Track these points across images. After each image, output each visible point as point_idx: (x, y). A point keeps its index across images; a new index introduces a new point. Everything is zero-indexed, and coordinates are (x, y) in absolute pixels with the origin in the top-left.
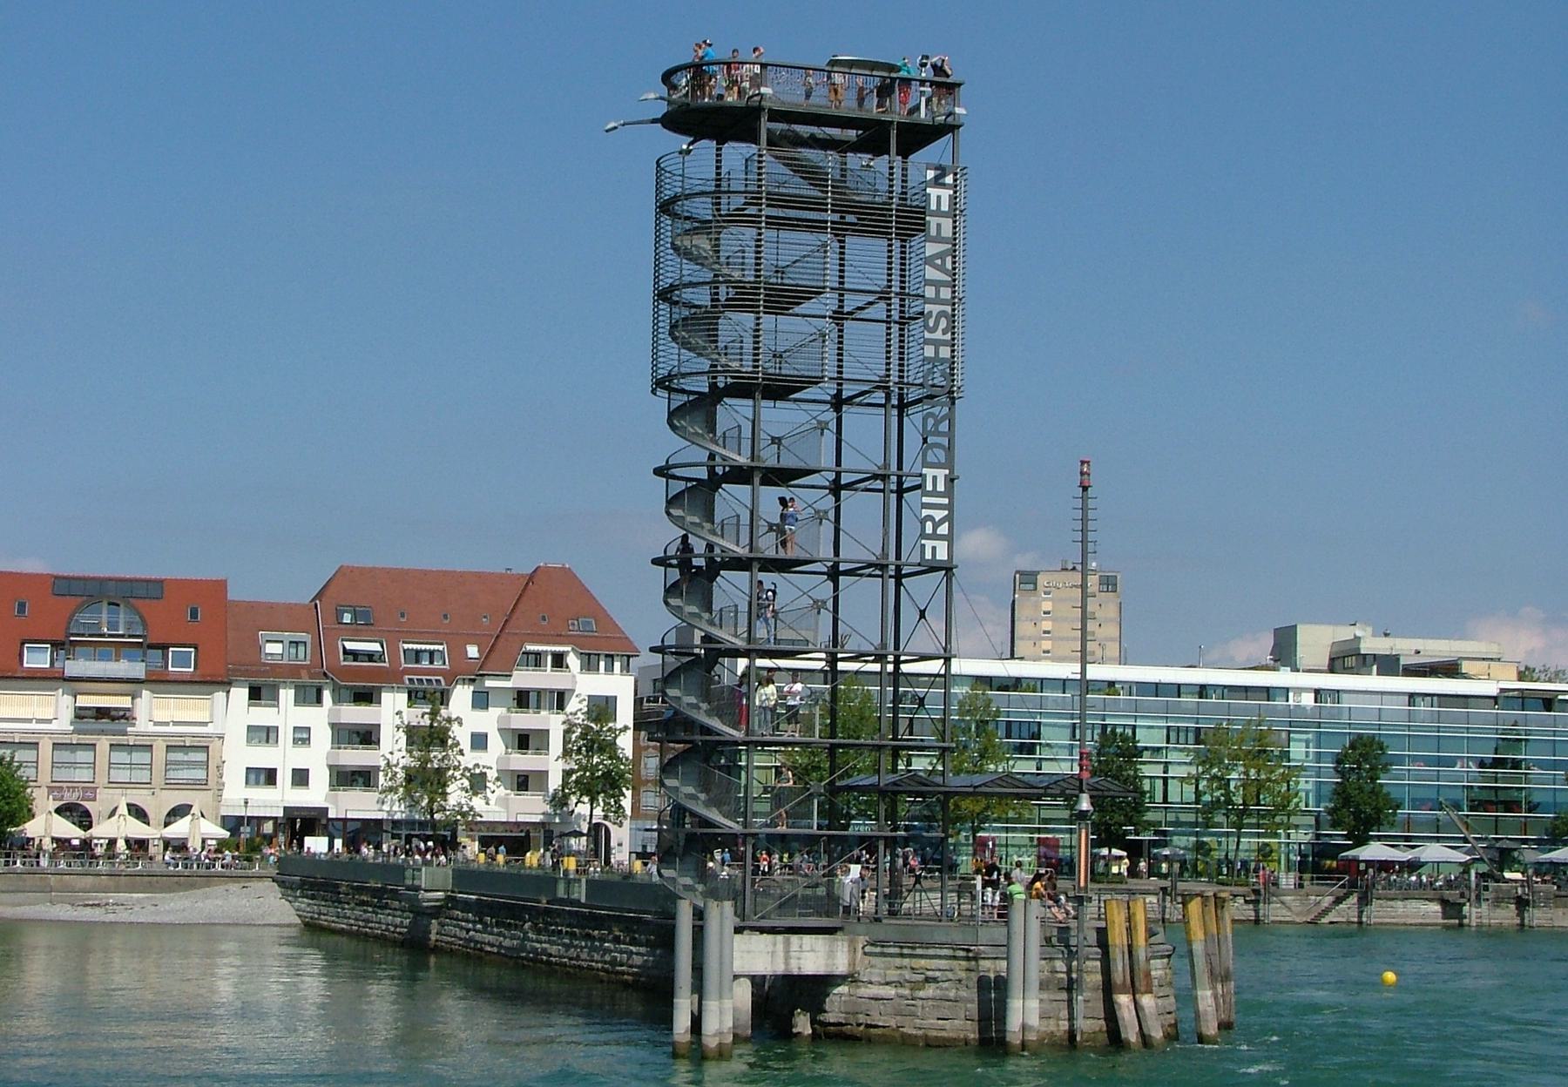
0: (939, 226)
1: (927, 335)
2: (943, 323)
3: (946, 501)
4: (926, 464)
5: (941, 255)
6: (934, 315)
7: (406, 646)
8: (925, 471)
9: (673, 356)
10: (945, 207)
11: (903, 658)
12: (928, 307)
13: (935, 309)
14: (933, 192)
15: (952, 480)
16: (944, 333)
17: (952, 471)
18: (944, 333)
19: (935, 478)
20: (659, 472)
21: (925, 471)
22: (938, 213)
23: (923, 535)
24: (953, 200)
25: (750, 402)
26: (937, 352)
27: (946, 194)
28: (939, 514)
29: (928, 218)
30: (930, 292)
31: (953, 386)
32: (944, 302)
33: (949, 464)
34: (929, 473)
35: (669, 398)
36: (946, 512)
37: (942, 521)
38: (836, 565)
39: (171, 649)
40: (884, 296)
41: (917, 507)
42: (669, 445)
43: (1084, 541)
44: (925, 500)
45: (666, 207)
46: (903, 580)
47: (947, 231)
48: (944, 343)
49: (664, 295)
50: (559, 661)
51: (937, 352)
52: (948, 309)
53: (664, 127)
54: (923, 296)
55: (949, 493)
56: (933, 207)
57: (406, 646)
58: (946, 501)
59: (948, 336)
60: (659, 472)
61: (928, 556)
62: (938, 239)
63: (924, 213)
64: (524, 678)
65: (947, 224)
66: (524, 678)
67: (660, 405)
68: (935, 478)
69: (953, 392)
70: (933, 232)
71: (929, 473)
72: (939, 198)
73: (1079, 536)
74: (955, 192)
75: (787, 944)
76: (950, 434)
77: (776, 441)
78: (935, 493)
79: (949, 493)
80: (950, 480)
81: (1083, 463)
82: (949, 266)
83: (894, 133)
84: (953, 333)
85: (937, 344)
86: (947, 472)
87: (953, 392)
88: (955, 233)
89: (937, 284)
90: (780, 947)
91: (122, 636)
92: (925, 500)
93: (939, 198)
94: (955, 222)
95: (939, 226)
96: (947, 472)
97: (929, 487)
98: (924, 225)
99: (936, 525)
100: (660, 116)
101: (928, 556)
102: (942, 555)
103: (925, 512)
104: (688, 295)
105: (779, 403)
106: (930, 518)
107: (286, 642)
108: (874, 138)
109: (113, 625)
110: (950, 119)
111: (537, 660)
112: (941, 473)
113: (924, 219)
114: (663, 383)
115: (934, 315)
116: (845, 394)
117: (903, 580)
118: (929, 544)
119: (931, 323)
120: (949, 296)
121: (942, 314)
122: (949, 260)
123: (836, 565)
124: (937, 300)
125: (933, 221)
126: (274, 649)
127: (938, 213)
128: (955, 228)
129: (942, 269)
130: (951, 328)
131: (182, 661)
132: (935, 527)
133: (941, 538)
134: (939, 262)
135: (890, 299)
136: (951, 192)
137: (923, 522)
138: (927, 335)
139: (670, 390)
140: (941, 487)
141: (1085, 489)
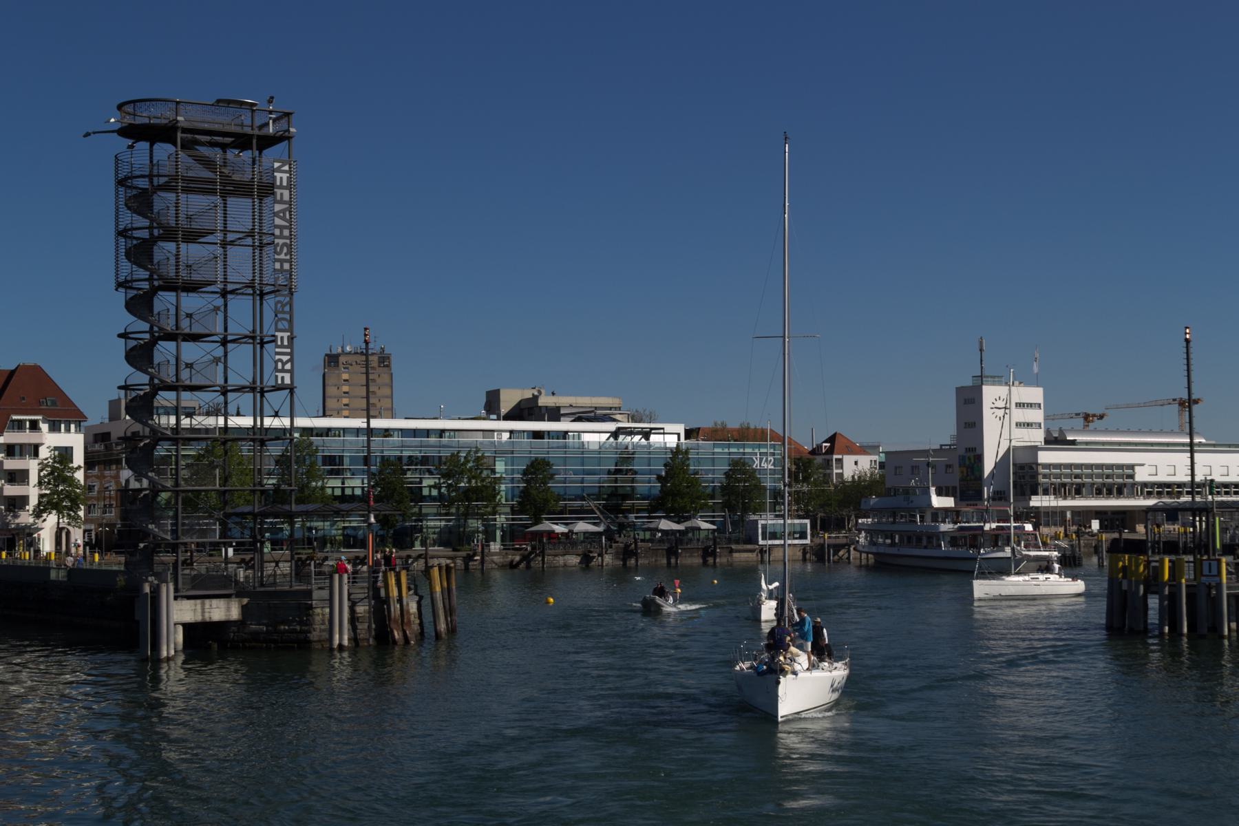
0: (282, 194)
1: (276, 257)
2: (285, 250)
3: (289, 350)
5: (283, 211)
8: (277, 334)
9: (128, 218)
10: (285, 183)
11: (266, 389)
13: (281, 241)
15: (292, 338)
16: (286, 255)
17: (292, 333)
18: (286, 255)
20: (120, 336)
21: (277, 334)
22: (281, 187)
23: (277, 370)
24: (289, 179)
25: (174, 294)
27: (285, 176)
28: (285, 358)
30: (277, 232)
32: (285, 238)
33: (291, 330)
34: (279, 334)
35: (126, 293)
36: (288, 357)
37: (287, 362)
38: (225, 337)
40: (251, 234)
41: (273, 354)
44: (277, 350)
45: (121, 182)
46: (265, 394)
47: (286, 197)
48: (286, 261)
49: (122, 233)
53: (119, 135)
55: (291, 345)
56: (278, 183)
58: (289, 350)
59: (288, 257)
60: (120, 336)
61: (280, 382)
62: (281, 202)
63: (273, 187)
65: (286, 193)
67: (121, 297)
68: (282, 338)
70: (278, 198)
71: (279, 334)
72: (281, 178)
74: (291, 175)
76: (291, 312)
77: (189, 316)
78: (282, 346)
79: (291, 345)
80: (291, 339)
81: (366, 329)
82: (288, 217)
83: (254, 141)
85: (282, 261)
88: (291, 198)
89: (281, 228)
92: (277, 350)
93: (281, 178)
94: (291, 192)
96: (289, 334)
97: (279, 343)
99: (284, 364)
100: (116, 128)
101: (280, 382)
102: (287, 381)
103: (278, 357)
104: (137, 234)
105: (190, 294)
106: (280, 360)
108: (242, 141)
110: (287, 134)
112: (286, 335)
114: (121, 285)
116: (228, 239)
117: (265, 394)
118: (280, 375)
119: (278, 249)
120: (288, 234)
121: (285, 244)
122: (287, 213)
123: (225, 337)
124: (281, 237)
125: (278, 192)
128: (291, 195)
129: (283, 218)
130: (290, 252)
132: (283, 366)
133: (287, 371)
134: (282, 215)
135: (254, 236)
137: (276, 362)
138: (276, 257)
139: (126, 288)
140: (286, 343)
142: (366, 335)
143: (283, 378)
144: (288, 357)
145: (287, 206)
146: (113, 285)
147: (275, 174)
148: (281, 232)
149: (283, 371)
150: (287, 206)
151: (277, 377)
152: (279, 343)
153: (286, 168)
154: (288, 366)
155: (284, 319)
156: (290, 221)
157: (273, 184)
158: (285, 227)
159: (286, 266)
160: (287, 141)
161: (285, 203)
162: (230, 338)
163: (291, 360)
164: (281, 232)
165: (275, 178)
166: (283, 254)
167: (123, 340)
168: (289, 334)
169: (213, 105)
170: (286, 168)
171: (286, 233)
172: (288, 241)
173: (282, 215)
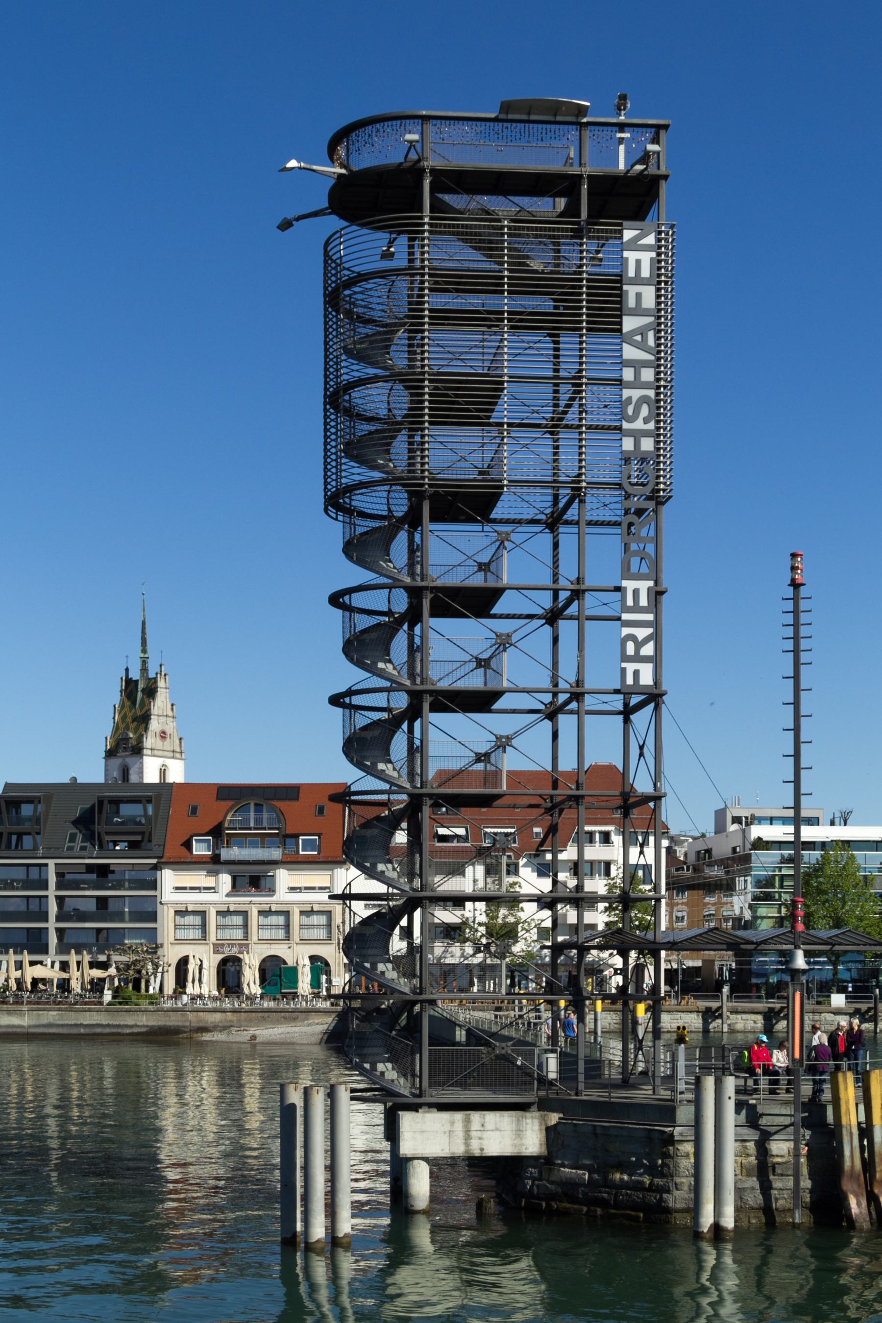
0: (639, 296)
2: (645, 411)
3: (650, 617)
5: (642, 331)
6: (634, 401)
8: (625, 583)
10: (645, 273)
13: (635, 394)
16: (646, 421)
18: (646, 421)
19: (636, 592)
21: (625, 583)
22: (638, 280)
23: (626, 658)
24: (656, 264)
26: (637, 444)
27: (646, 258)
28: (642, 633)
29: (625, 287)
30: (628, 374)
31: (658, 484)
32: (646, 386)
36: (650, 631)
37: (646, 640)
48: (646, 434)
51: (637, 444)
52: (651, 393)
54: (621, 380)
56: (631, 273)
58: (650, 617)
59: (651, 426)
61: (630, 681)
62: (638, 311)
63: (620, 282)
65: (649, 295)
68: (636, 592)
69: (658, 491)
70: (631, 303)
71: (629, 585)
72: (638, 262)
74: (659, 254)
78: (636, 609)
80: (657, 594)
81: (794, 556)
82: (651, 341)
84: (658, 422)
85: (637, 435)
86: (651, 583)
87: (658, 491)
88: (659, 303)
89: (637, 365)
93: (638, 262)
94: (658, 290)
96: (651, 583)
97: (630, 602)
98: (620, 296)
99: (639, 645)
101: (630, 681)
102: (647, 678)
103: (626, 631)
106: (632, 638)
110: (651, 170)
112: (644, 586)
113: (620, 289)
115: (634, 401)
118: (630, 667)
121: (644, 399)
122: (651, 335)
124: (637, 384)
125: (631, 291)
128: (658, 297)
130: (656, 415)
133: (645, 659)
136: (653, 254)
140: (644, 602)
141: (795, 585)
142: (793, 568)
143: (636, 673)
144: (650, 631)
145: (652, 319)
147: (626, 254)
148: (637, 375)
149: (638, 658)
150: (652, 319)
151: (623, 671)
152: (630, 602)
157: (621, 276)
158: (645, 364)
159: (647, 444)
161: (645, 313)
163: (656, 637)
164: (637, 375)
165: (624, 262)
166: (640, 420)
169: (496, 120)
170: (650, 240)
171: (648, 375)
173: (638, 338)
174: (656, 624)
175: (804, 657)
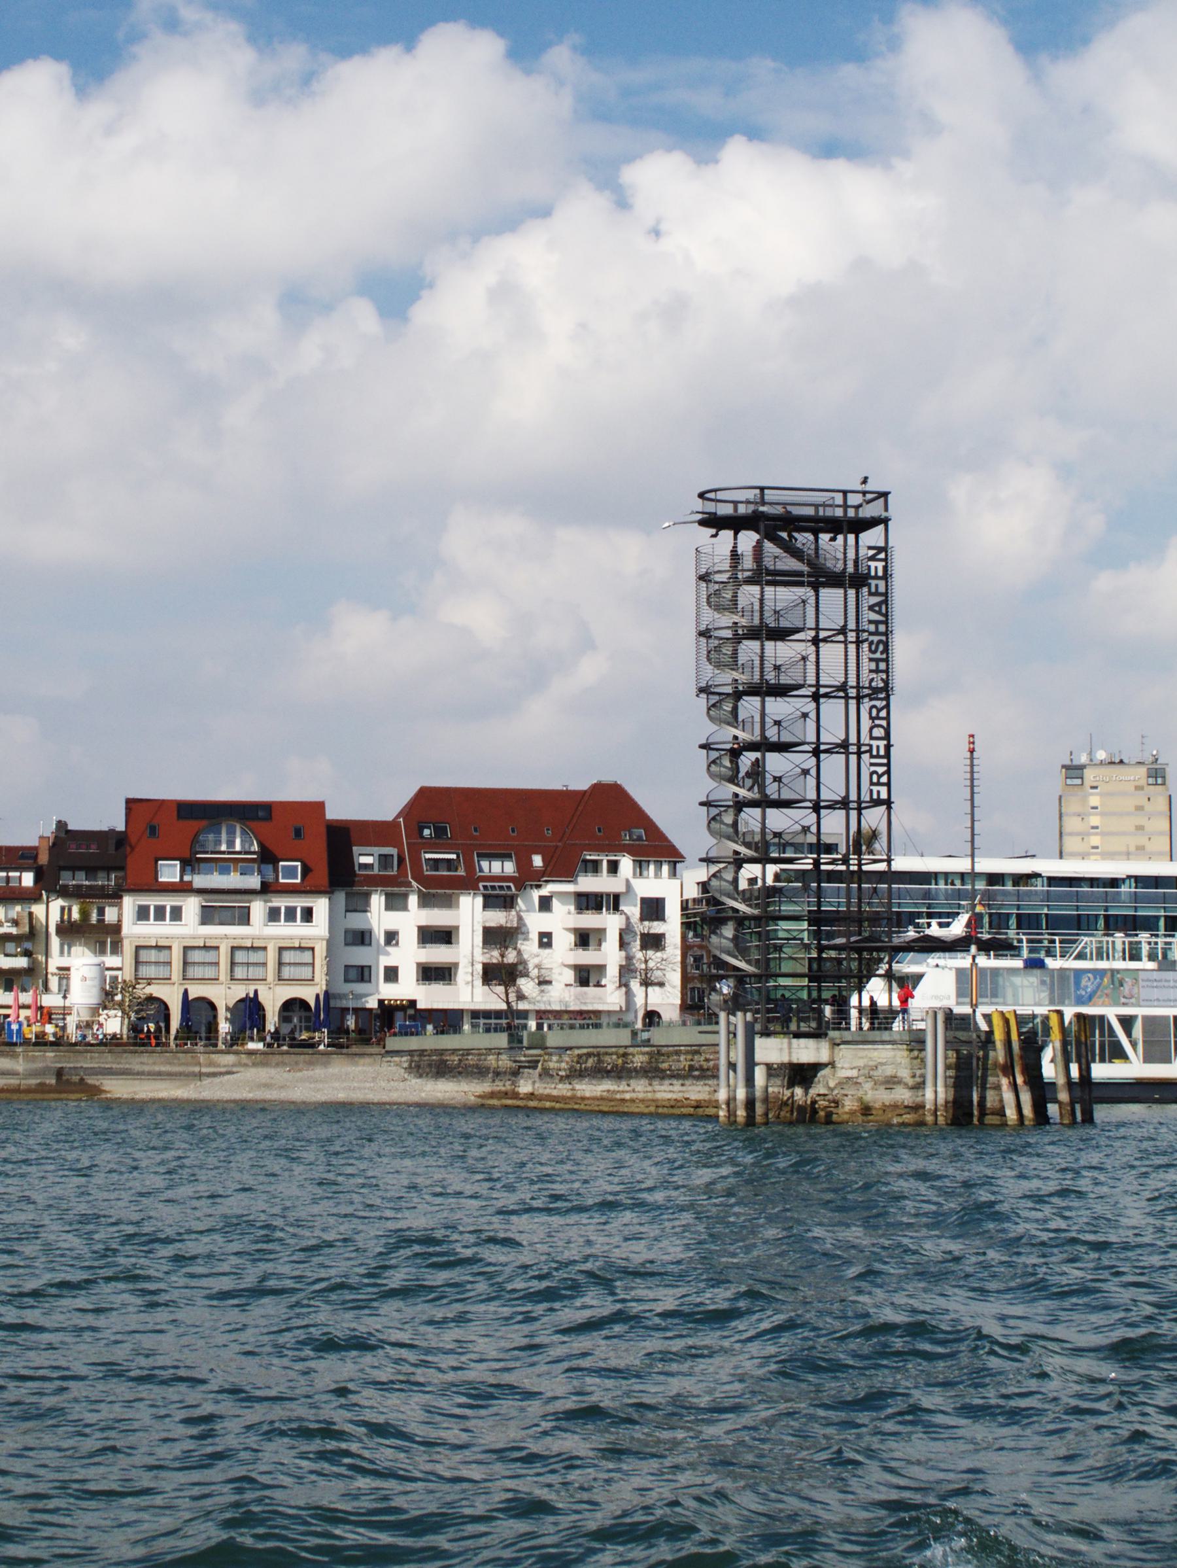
0: (877, 586)
2: (881, 648)
3: (885, 761)
4: (872, 738)
5: (879, 604)
7: (428, 856)
10: (880, 573)
12: (871, 638)
13: (875, 639)
14: (873, 564)
16: (882, 653)
17: (889, 741)
18: (882, 653)
19: (878, 747)
20: (702, 747)
21: (872, 742)
22: (876, 577)
23: (872, 784)
24: (885, 568)
25: (758, 698)
27: (880, 565)
28: (881, 770)
33: (887, 736)
36: (885, 768)
37: (883, 774)
39: (281, 863)
42: (707, 729)
43: (972, 786)
47: (882, 589)
48: (882, 660)
49: (705, 634)
50: (614, 868)
56: (873, 573)
57: (428, 856)
58: (885, 761)
60: (702, 747)
61: (875, 796)
62: (877, 594)
64: (588, 883)
65: (882, 584)
66: (588, 883)
68: (878, 747)
70: (873, 590)
71: (874, 743)
73: (968, 783)
75: (790, 1044)
76: (888, 718)
77: (778, 723)
78: (878, 756)
82: (884, 611)
89: (876, 623)
90: (785, 1045)
91: (223, 853)
95: (877, 586)
96: (885, 742)
97: (874, 753)
99: (880, 776)
101: (875, 796)
102: (884, 796)
103: (873, 769)
105: (778, 699)
107: (376, 855)
109: (231, 843)
111: (595, 867)
112: (882, 743)
114: (704, 690)
118: (875, 789)
119: (873, 647)
121: (880, 642)
124: (876, 633)
125: (873, 583)
126: (364, 860)
127: (876, 577)
129: (879, 613)
131: (291, 872)
133: (883, 784)
140: (882, 752)
141: (972, 751)
143: (878, 792)
144: (885, 768)
145: (883, 598)
146: (694, 691)
149: (879, 784)
150: (883, 598)
151: (871, 791)
153: (882, 556)
154: (884, 779)
155: (881, 726)
156: (886, 615)
160: (882, 527)
162: (822, 747)
163: (888, 772)
167: (705, 751)
168: (885, 742)
172: (884, 638)
174: (888, 765)
175: (976, 790)
